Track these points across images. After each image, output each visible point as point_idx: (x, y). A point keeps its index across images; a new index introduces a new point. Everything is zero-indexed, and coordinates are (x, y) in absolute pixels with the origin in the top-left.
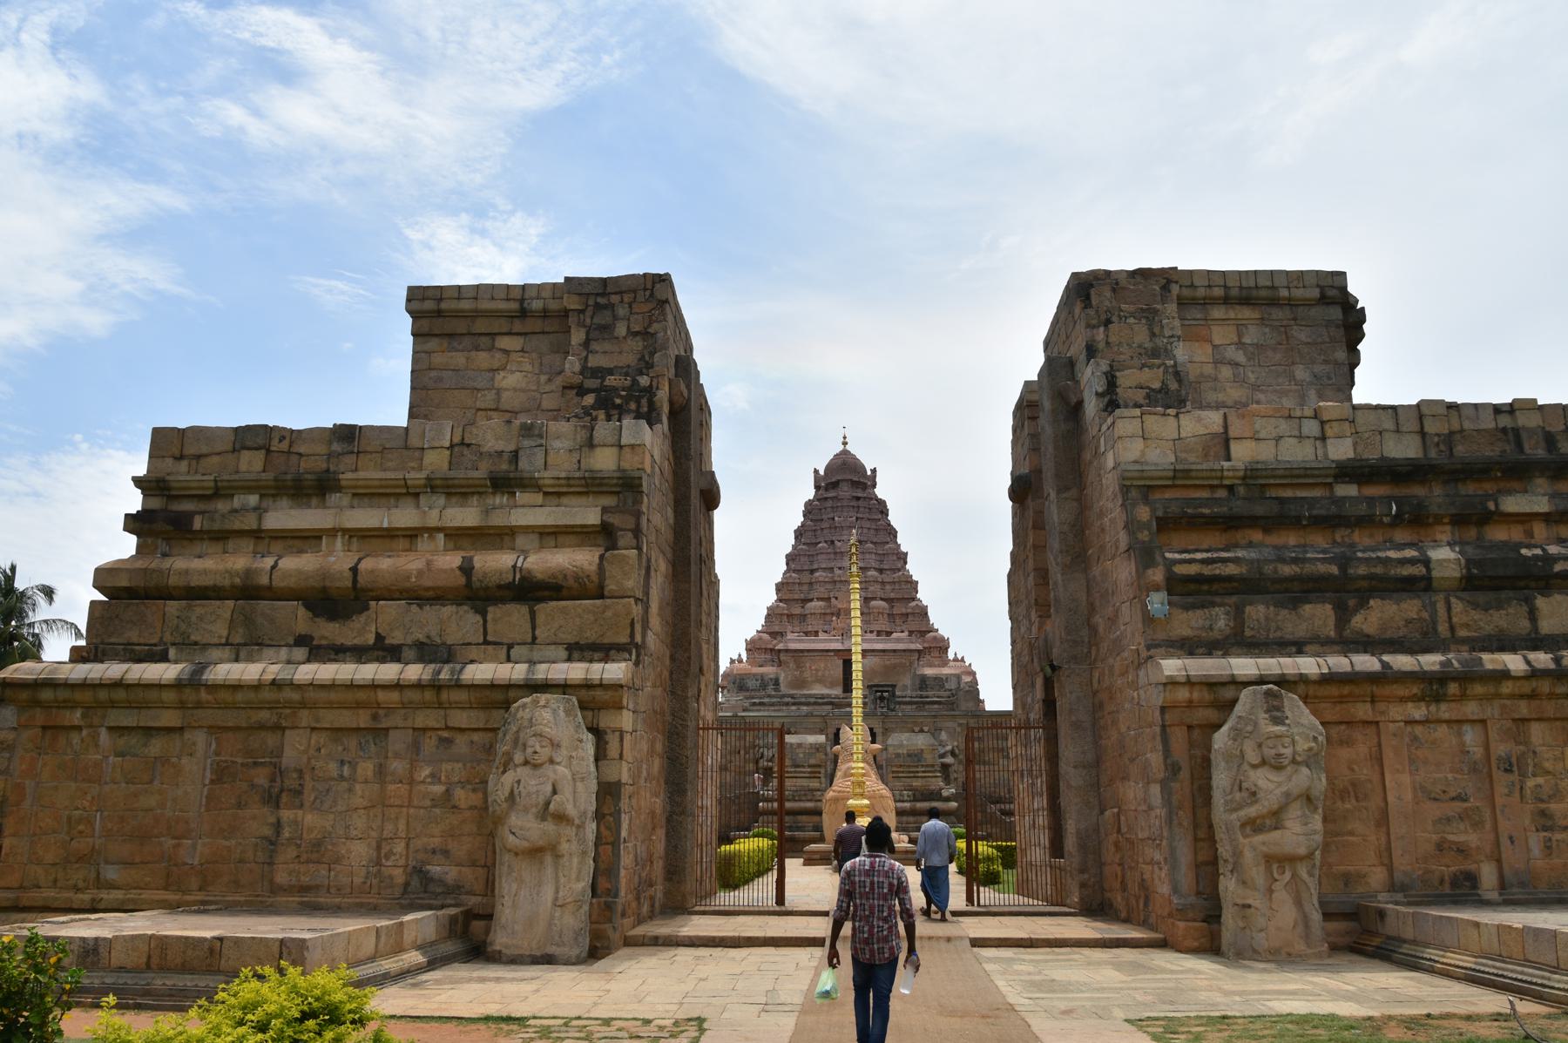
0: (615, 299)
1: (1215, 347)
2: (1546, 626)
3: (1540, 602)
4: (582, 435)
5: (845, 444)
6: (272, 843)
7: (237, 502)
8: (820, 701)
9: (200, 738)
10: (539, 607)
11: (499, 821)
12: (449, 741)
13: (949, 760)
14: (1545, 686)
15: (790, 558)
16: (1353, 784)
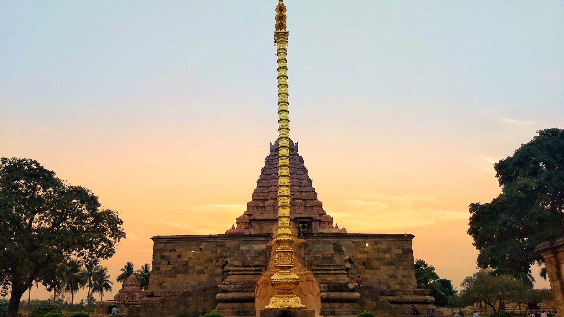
13: (348, 265)
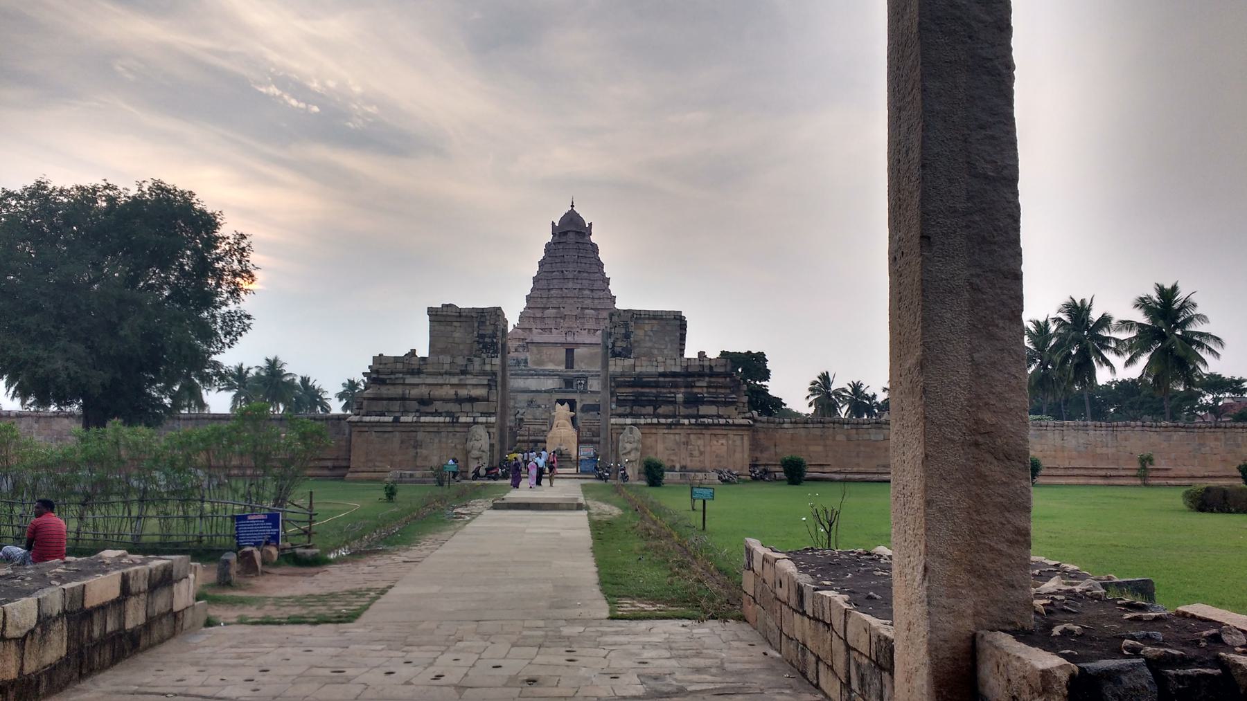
0: (486, 314)
1: (645, 331)
2: (700, 413)
3: (700, 407)
4: (482, 361)
5: (572, 206)
6: (415, 457)
7: (397, 376)
8: (552, 373)
9: (397, 433)
10: (474, 404)
11: (469, 452)
12: (455, 435)
14: (693, 427)
15: (535, 280)
16: (651, 447)
